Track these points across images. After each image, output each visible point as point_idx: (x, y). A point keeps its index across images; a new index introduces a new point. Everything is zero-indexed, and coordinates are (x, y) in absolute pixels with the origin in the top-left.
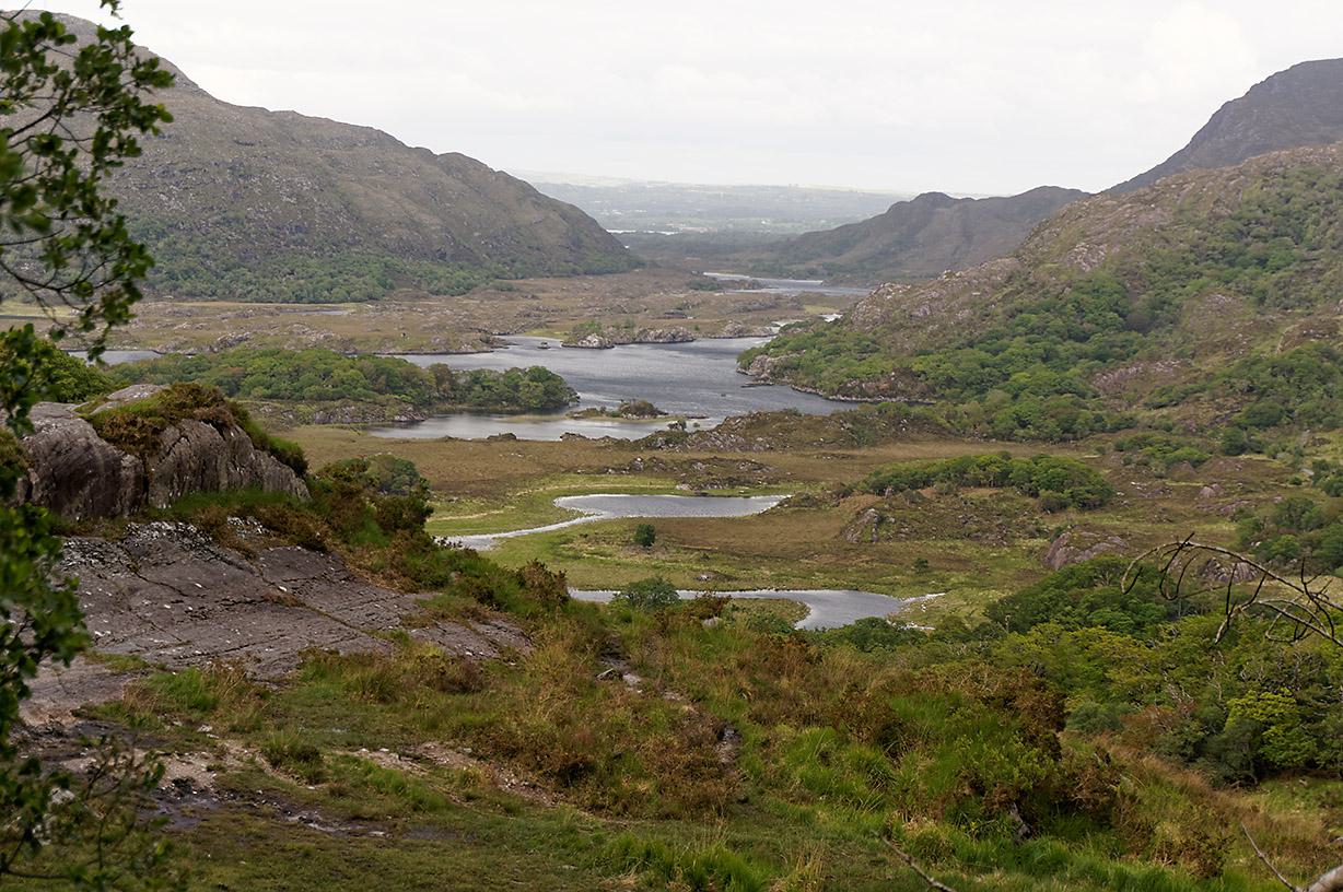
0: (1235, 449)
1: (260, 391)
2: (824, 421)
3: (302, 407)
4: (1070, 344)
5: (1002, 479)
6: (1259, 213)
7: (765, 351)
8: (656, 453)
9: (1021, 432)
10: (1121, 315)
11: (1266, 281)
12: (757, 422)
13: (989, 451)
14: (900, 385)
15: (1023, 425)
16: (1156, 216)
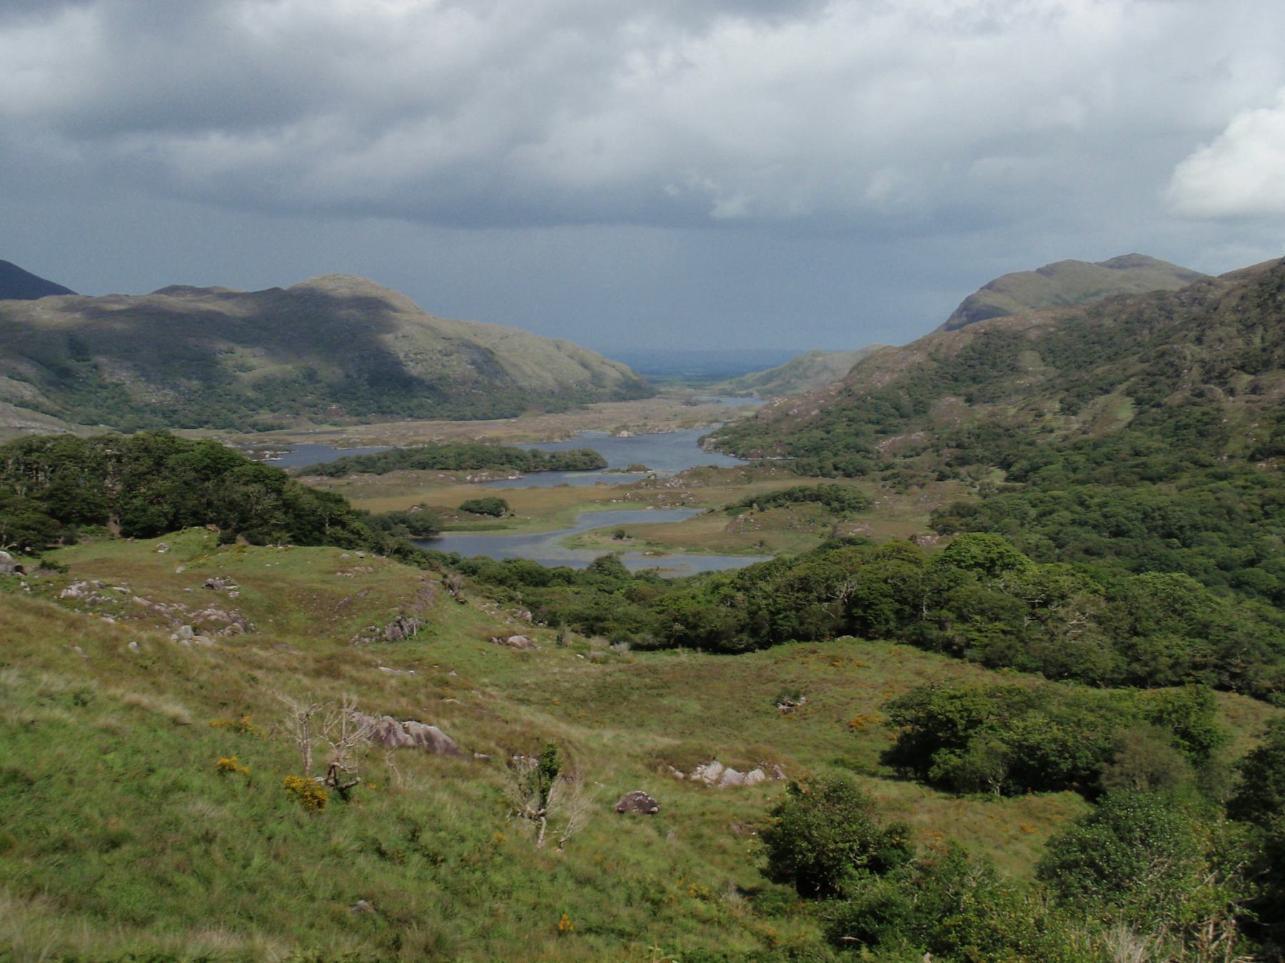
0: (942, 478)
1: (440, 466)
2: (727, 471)
3: (461, 473)
4: (870, 426)
5: (816, 497)
6: (972, 353)
7: (711, 436)
8: (640, 491)
9: (835, 472)
10: (898, 410)
11: (974, 389)
12: (696, 473)
13: (812, 483)
14: (779, 451)
15: (836, 468)
16: (919, 357)
